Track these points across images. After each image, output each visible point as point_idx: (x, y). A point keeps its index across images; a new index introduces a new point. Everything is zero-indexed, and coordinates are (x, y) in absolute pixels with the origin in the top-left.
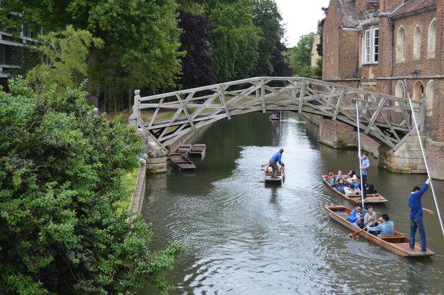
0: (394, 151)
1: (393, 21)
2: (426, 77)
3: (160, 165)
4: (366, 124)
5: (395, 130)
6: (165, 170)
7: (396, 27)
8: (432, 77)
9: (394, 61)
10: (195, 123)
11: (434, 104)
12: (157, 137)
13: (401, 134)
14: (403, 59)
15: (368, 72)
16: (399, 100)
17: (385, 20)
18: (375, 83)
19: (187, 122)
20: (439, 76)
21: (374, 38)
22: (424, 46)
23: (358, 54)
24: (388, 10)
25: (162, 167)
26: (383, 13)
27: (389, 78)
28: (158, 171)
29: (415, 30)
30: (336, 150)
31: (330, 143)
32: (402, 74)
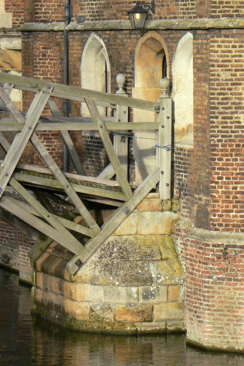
0: (80, 264)
2: (175, 23)
8: (189, 25)
11: (197, 111)
20: (210, 23)
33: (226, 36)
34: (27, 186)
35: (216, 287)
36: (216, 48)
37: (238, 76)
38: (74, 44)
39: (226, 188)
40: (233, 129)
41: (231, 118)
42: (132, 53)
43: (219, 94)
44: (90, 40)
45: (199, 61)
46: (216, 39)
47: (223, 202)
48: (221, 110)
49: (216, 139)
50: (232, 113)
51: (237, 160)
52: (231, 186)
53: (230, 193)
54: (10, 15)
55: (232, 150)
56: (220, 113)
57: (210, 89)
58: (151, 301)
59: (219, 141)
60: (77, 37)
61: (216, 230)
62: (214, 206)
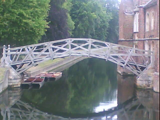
0: (138, 77)
1: (145, 9)
3: (17, 83)
4: (124, 63)
5: (139, 66)
6: (20, 86)
7: (146, 12)
9: (145, 31)
10: (35, 62)
12: (15, 69)
13: (143, 69)
14: (148, 30)
16: (147, 51)
17: (142, 9)
19: (30, 61)
21: (138, 18)
24: (143, 4)
25: (17, 85)
26: (141, 6)
27: (143, 39)
28: (15, 86)
29: (152, 14)
30: (122, 76)
31: (120, 72)
34: (130, 64)
38: (145, 42)
42: (151, 43)
54: (137, 37)
58: (149, 84)
60: (145, 41)
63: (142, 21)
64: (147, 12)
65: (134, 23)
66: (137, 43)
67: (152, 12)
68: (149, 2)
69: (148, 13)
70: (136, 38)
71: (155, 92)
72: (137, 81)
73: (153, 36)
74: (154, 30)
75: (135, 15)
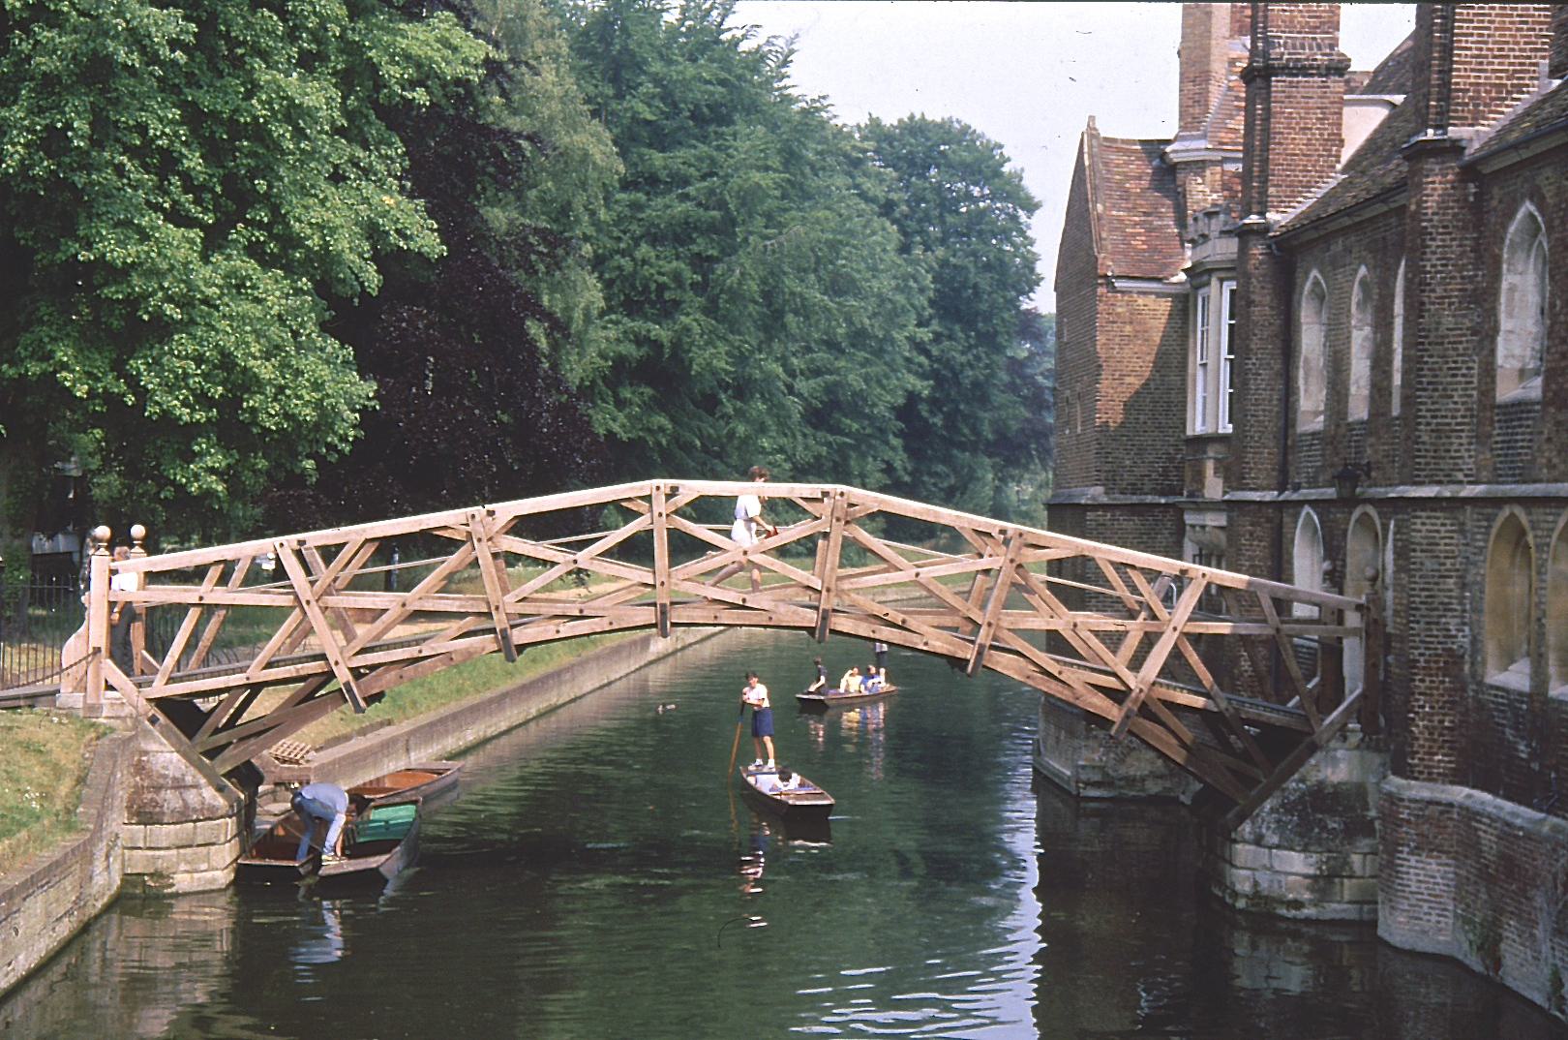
7: (1299, 274)
15: (1199, 477)
18: (1221, 520)
22: (1380, 362)
23: (1183, 391)
27: (1270, 496)
32: (1313, 483)
33: (1434, 510)
35: (1413, 859)
36: (1419, 527)
37: (1448, 566)
39: (1430, 721)
40: (1442, 640)
41: (1438, 623)
43: (1423, 590)
44: (1303, 514)
45: (1400, 544)
46: (1419, 514)
47: (1426, 740)
48: (1425, 613)
49: (1416, 652)
50: (1440, 616)
51: (1443, 682)
52: (1436, 718)
53: (1434, 728)
54: (1220, 482)
55: (1439, 669)
56: (1423, 616)
57: (1410, 583)
59: (1421, 655)
60: (1291, 511)
61: (1416, 779)
62: (1412, 746)
63: (1261, 345)
64: (1307, 274)
65: (1195, 359)
66: (1222, 528)
67: (1356, 271)
68: (1325, 188)
69: (1316, 283)
70: (1208, 482)
71: (1387, 944)
72: (1239, 846)
73: (1368, 475)
74: (1369, 426)
75: (1202, 292)
